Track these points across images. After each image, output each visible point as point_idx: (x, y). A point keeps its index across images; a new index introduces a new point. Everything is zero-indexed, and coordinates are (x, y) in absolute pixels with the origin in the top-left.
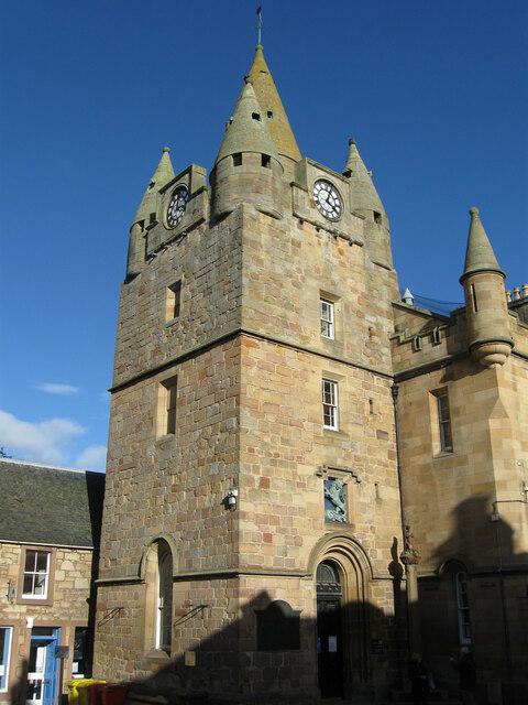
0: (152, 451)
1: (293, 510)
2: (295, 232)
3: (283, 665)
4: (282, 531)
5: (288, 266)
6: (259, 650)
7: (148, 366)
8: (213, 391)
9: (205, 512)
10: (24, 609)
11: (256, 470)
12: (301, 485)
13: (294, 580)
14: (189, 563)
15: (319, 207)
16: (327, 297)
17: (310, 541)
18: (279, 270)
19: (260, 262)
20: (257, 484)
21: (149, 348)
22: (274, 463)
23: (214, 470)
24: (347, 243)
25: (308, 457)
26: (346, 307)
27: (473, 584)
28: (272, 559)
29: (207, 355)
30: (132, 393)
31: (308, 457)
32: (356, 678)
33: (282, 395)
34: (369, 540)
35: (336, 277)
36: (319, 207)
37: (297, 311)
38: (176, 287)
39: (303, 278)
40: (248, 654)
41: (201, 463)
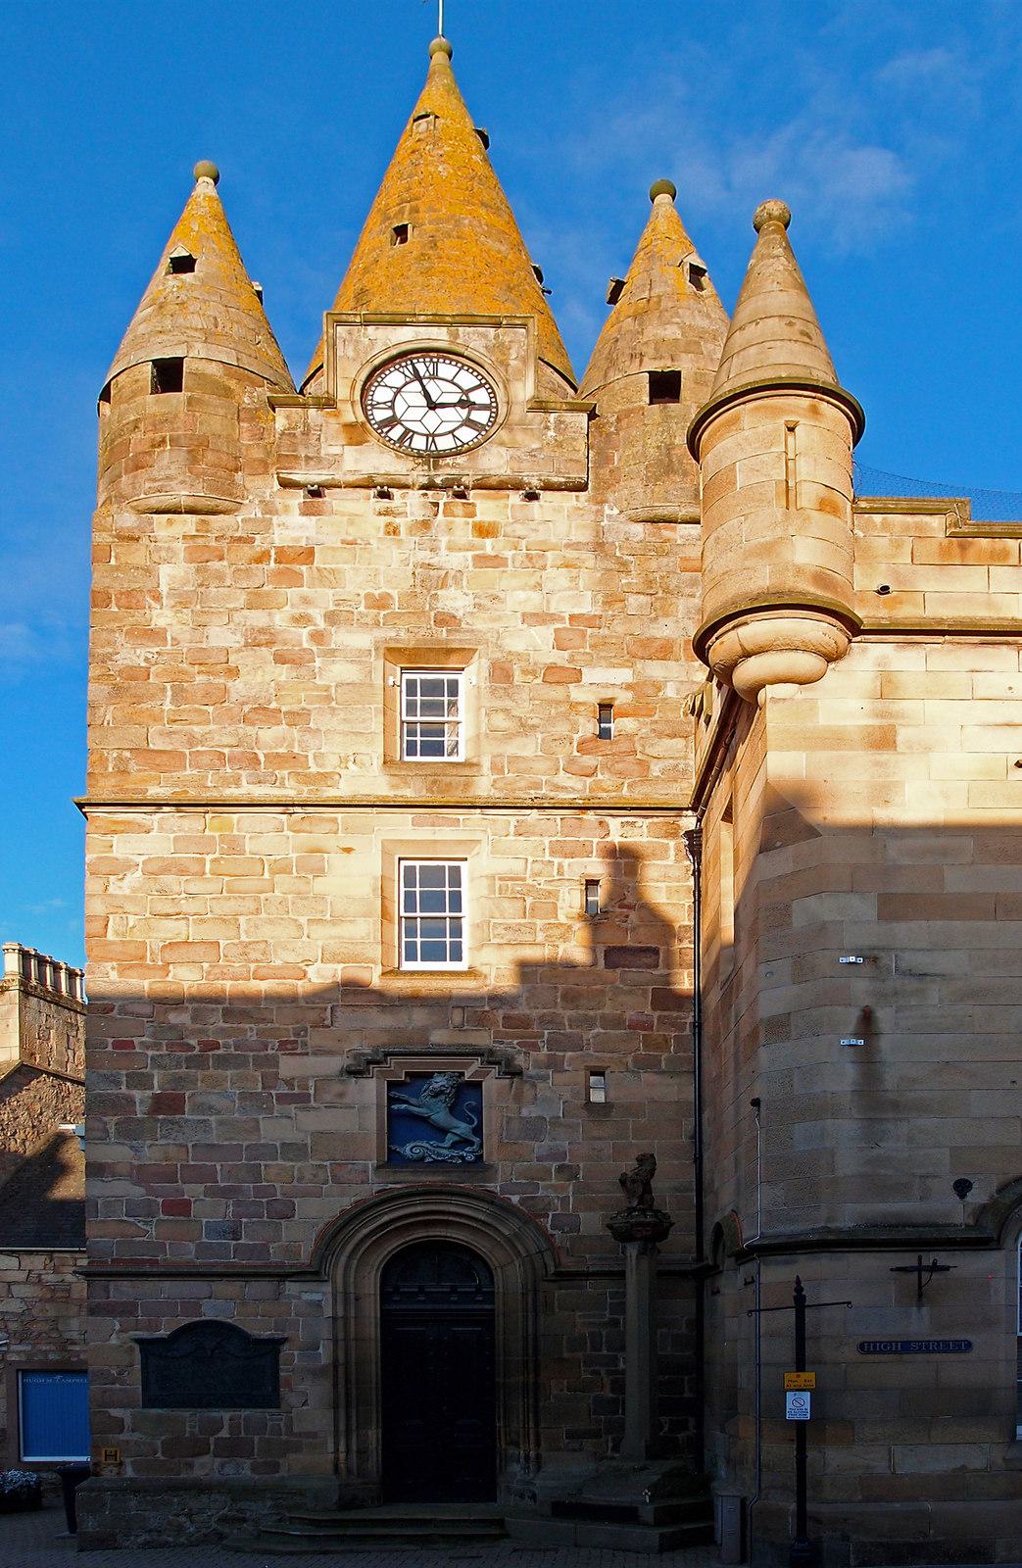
1: (261, 1151)
2: (292, 525)
3: (224, 1433)
5: (258, 618)
6: (149, 1402)
11: (140, 1081)
12: (303, 1099)
13: (262, 1288)
15: (396, 433)
18: (221, 636)
19: (155, 635)
20: (140, 1111)
22: (198, 1062)
24: (515, 498)
26: (501, 674)
28: (192, 1246)
31: (315, 1039)
33: (230, 921)
35: (454, 600)
36: (396, 433)
37: (297, 718)
39: (318, 637)
40: (115, 1412)
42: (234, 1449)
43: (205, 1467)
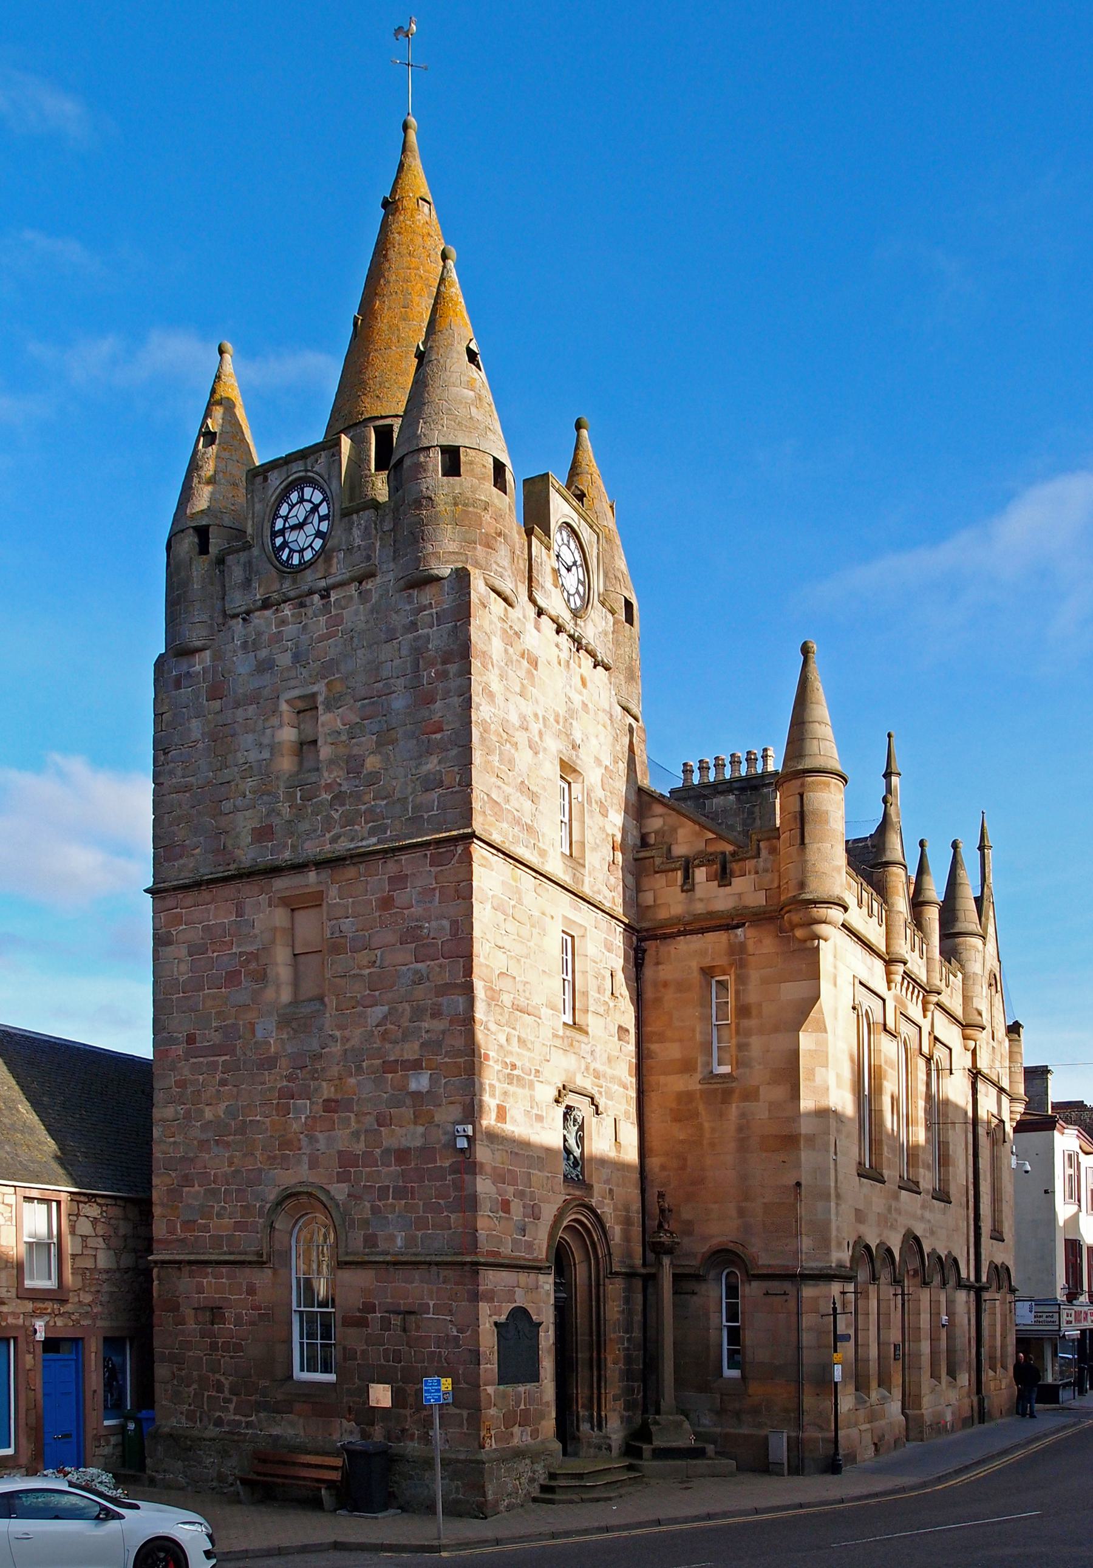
0: (268, 1032)
3: (522, 1407)
4: (520, 1195)
7: (247, 854)
8: (411, 935)
9: (402, 1155)
10: (29, 1306)
14: (370, 1241)
16: (568, 769)
17: (549, 1212)
21: (245, 823)
23: (420, 1082)
25: (547, 1071)
27: (751, 1291)
29: (392, 867)
30: (215, 912)
32: (585, 1427)
34: (607, 1210)
38: (307, 707)
41: (389, 1067)
42: (525, 1419)
43: (520, 1437)
